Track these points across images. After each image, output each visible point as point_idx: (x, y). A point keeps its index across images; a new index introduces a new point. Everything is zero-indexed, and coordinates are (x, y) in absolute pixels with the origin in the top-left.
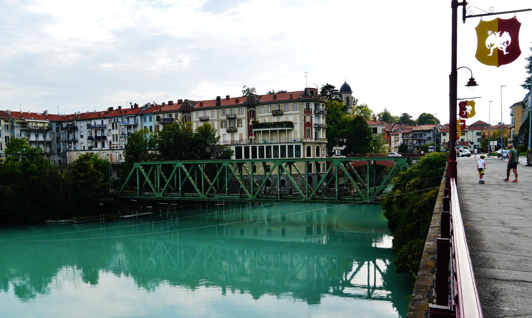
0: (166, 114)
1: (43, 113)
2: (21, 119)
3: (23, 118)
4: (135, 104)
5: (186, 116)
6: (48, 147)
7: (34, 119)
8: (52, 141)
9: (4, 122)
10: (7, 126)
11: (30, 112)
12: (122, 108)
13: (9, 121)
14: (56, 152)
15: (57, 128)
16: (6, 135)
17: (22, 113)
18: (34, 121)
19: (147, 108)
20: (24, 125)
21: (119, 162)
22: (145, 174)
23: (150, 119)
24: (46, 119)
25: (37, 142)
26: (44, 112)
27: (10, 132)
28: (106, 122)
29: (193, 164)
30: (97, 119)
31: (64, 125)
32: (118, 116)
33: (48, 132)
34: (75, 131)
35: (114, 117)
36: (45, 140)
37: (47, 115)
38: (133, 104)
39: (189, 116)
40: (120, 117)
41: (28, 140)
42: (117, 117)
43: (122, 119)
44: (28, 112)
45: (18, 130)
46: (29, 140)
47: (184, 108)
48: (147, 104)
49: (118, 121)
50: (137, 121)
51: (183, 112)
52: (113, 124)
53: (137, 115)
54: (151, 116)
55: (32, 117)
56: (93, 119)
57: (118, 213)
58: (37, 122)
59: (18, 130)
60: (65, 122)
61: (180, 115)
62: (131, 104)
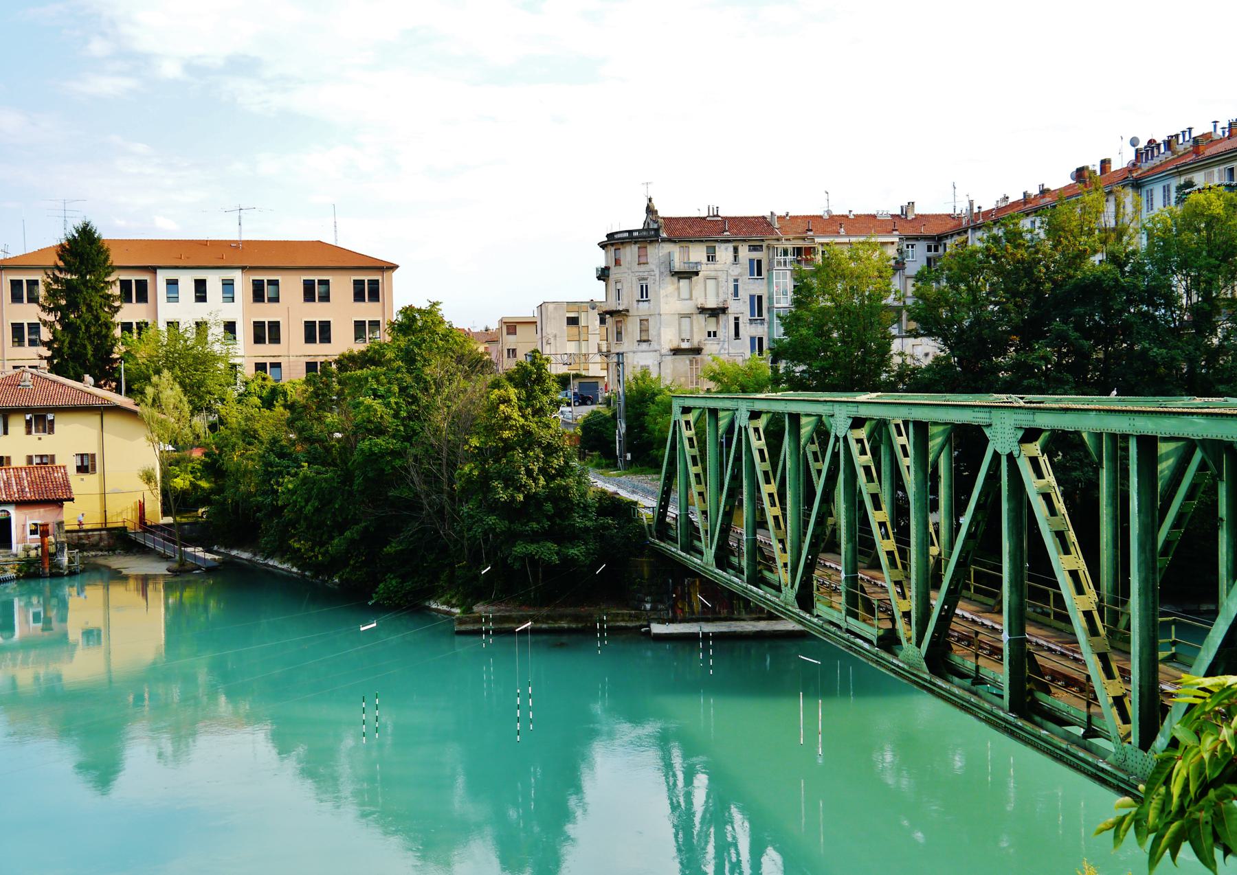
0: (1216, 170)
1: (899, 212)
2: (804, 239)
7: (847, 235)
9: (749, 250)
10: (759, 262)
11: (852, 213)
12: (1115, 166)
13: (764, 245)
15: (929, 260)
16: (753, 293)
18: (846, 240)
19: (1173, 153)
23: (1164, 191)
26: (902, 207)
27: (765, 281)
44: (847, 213)
45: (785, 276)
48: (1177, 136)
54: (1168, 186)
57: (645, 610)
60: (952, 236)
62: (1134, 146)
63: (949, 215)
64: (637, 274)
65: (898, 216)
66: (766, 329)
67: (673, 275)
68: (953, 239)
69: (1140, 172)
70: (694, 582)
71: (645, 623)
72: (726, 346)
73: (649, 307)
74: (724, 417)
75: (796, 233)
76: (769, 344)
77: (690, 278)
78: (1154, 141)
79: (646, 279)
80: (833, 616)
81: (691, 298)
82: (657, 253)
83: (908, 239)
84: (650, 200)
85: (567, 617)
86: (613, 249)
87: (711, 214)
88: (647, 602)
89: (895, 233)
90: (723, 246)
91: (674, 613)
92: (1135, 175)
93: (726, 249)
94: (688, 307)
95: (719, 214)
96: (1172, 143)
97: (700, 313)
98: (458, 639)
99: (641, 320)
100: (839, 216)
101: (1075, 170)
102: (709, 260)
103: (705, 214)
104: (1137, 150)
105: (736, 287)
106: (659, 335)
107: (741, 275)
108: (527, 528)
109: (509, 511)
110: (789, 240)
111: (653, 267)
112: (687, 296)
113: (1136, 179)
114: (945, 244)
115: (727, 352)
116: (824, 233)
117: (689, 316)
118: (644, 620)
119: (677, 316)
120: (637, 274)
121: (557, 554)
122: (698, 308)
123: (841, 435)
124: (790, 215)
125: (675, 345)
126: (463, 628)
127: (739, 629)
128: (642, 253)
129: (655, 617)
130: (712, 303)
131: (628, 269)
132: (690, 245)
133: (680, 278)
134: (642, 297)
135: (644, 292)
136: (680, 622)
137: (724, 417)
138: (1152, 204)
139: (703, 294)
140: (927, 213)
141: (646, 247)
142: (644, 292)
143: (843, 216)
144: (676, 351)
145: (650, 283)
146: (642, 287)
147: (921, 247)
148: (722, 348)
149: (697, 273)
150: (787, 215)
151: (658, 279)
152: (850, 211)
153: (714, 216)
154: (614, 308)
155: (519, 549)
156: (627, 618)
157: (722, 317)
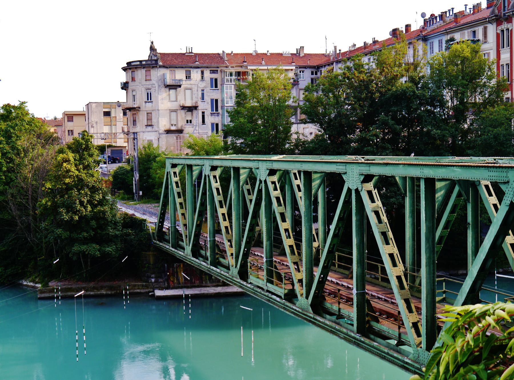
0: (466, 31)
1: (295, 52)
5: (503, 31)
7: (266, 65)
9: (210, 73)
10: (216, 80)
11: (269, 52)
12: (413, 28)
13: (219, 70)
15: (312, 79)
16: (212, 98)
17: (269, 54)
18: (266, 68)
19: (444, 22)
23: (439, 43)
24: (290, 64)
27: (220, 90)
37: (302, 55)
39: (510, 29)
44: (266, 52)
45: (231, 89)
48: (446, 12)
54: (441, 40)
55: (264, 62)
57: (151, 282)
59: (231, 88)
60: (325, 66)
61: (492, 29)
62: (423, 17)
63: (323, 54)
64: (145, 86)
65: (295, 54)
66: (220, 119)
67: (166, 87)
68: (326, 68)
69: (426, 32)
70: (180, 266)
71: (152, 290)
72: (197, 128)
73: (152, 106)
74: (196, 170)
75: (237, 63)
76: (222, 127)
77: (176, 89)
78: (434, 15)
79: (150, 89)
80: (259, 283)
81: (176, 101)
82: (157, 74)
83: (300, 68)
84: (152, 43)
85: (105, 287)
86: (130, 71)
87: (188, 52)
88: (153, 278)
89: (293, 64)
90: (195, 70)
91: (168, 284)
92: (423, 33)
93: (197, 72)
94: (175, 106)
95: (193, 52)
96: (443, 16)
97: (182, 109)
98: (40, 302)
99: (147, 113)
100: (261, 54)
101: (392, 30)
102: (187, 78)
103: (185, 52)
104: (425, 20)
105: (203, 94)
106: (158, 122)
107: (206, 87)
108: (81, 236)
109: (69, 225)
110: (233, 67)
111: (154, 82)
112: (174, 99)
113: (424, 36)
114: (321, 71)
115: (198, 132)
116: (253, 64)
117: (175, 111)
118: (151, 288)
119: (168, 111)
120: (145, 86)
121: (99, 250)
122: (181, 107)
123: (263, 179)
124: (233, 53)
125: (167, 128)
126: (43, 295)
127: (206, 292)
128: (148, 73)
129: (157, 286)
130: (188, 104)
131: (140, 83)
132: (176, 70)
133: (170, 89)
134: (148, 100)
135: (149, 96)
136: (172, 289)
137: (196, 170)
138: (433, 50)
139: (184, 99)
141: (150, 71)
142: (149, 96)
143: (264, 54)
144: (168, 132)
145: (152, 91)
146: (148, 94)
147: (308, 72)
148: (195, 129)
150: (232, 53)
151: (157, 89)
153: (190, 53)
154: (131, 106)
155: (76, 248)
156: (140, 287)
157: (195, 112)
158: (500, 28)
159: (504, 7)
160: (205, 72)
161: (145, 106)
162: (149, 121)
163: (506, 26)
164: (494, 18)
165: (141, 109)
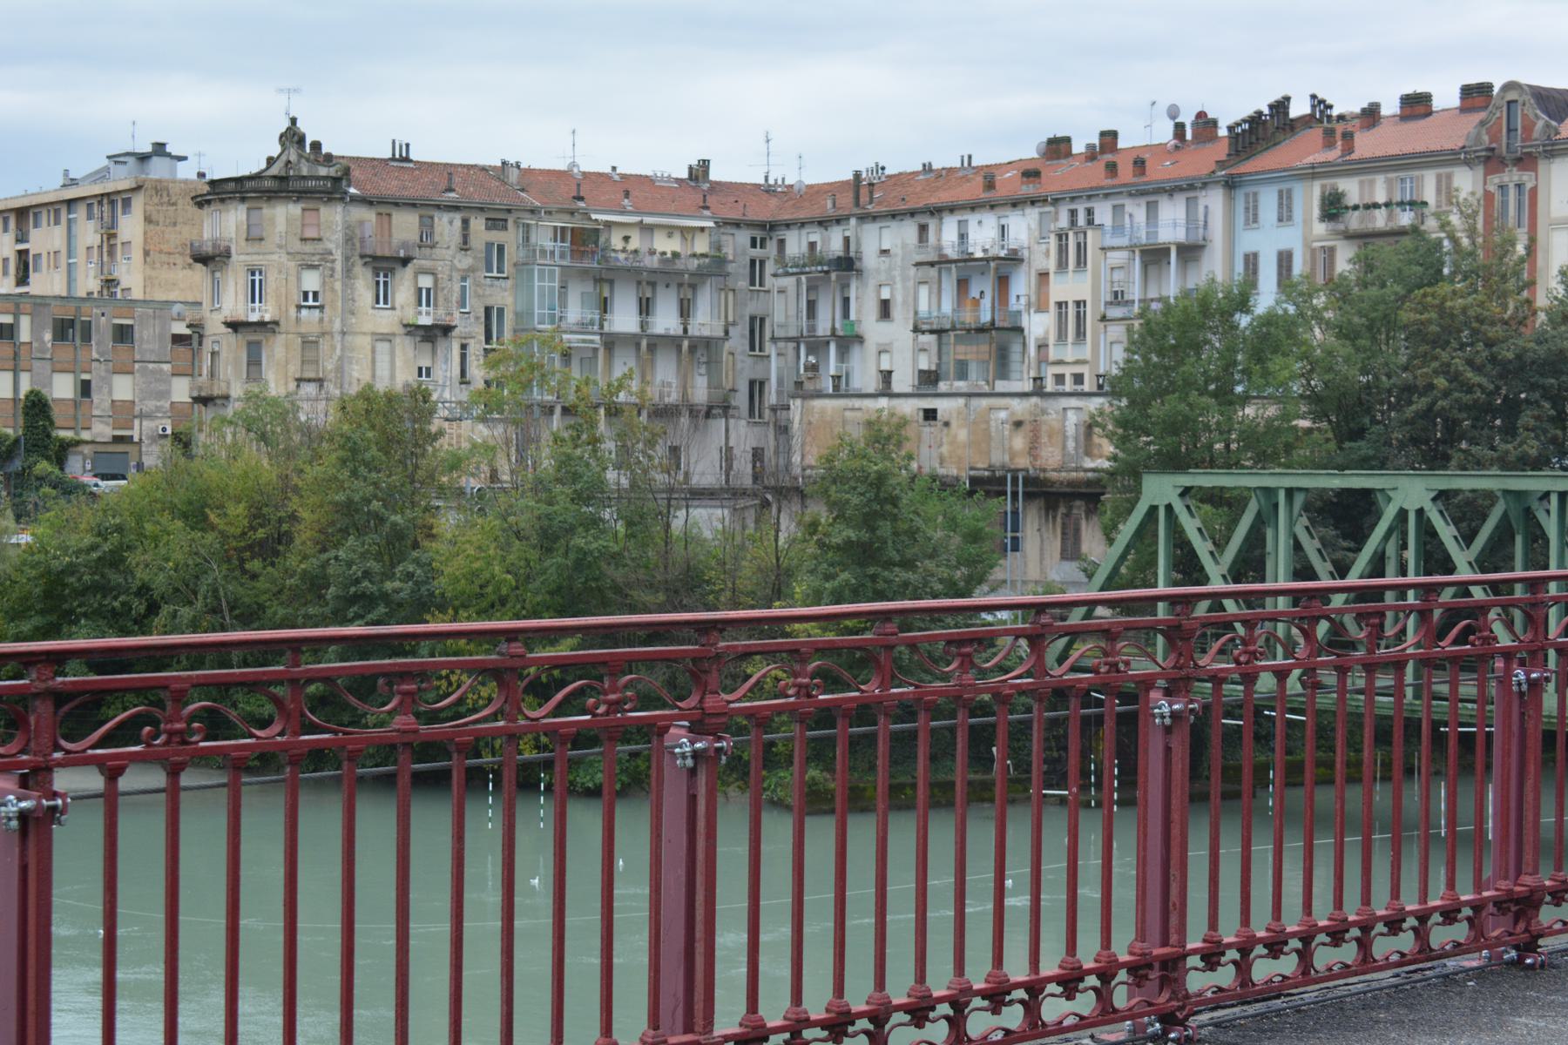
3: (581, 204)
4: (1201, 115)
6: (703, 370)
8: (722, 334)
9: (488, 228)
10: (501, 249)
11: (618, 171)
14: (741, 400)
16: (489, 302)
20: (584, 240)
21: (1076, 470)
22: (1202, 548)
25: (644, 343)
26: (691, 168)
28: (1022, 227)
29: (1506, 492)
30: (973, 207)
31: (796, 244)
32: (1091, 189)
33: (704, 283)
34: (848, 278)
35: (1073, 199)
36: (685, 331)
38: (1187, 118)
40: (1107, 196)
41: (601, 327)
42: (1089, 197)
43: (1115, 207)
44: (608, 170)
46: (606, 329)
47: (1495, 137)
49: (1090, 222)
50: (1201, 223)
51: (1491, 160)
52: (1061, 236)
53: (1205, 185)
54: (1289, 191)
56: (952, 209)
58: (648, 229)
59: (552, 273)
62: (1173, 117)
63: (757, 186)
64: (298, 257)
73: (321, 320)
78: (1205, 114)
84: (294, 121)
87: (397, 156)
89: (706, 213)
93: (451, 223)
95: (413, 156)
97: (408, 334)
101: (1045, 140)
107: (472, 269)
111: (331, 246)
114: (782, 242)
117: (387, 338)
119: (368, 339)
122: (405, 326)
128: (255, 213)
138: (1256, 216)
140: (728, 180)
141: (317, 210)
147: (743, 237)
149: (405, 262)
152: (614, 168)
154: (243, 318)
157: (441, 344)
158: (1495, 179)
159: (1511, 130)
160: (473, 222)
161: (298, 320)
162: (306, 367)
163: (1516, 178)
164: (1484, 153)
165: (283, 327)
